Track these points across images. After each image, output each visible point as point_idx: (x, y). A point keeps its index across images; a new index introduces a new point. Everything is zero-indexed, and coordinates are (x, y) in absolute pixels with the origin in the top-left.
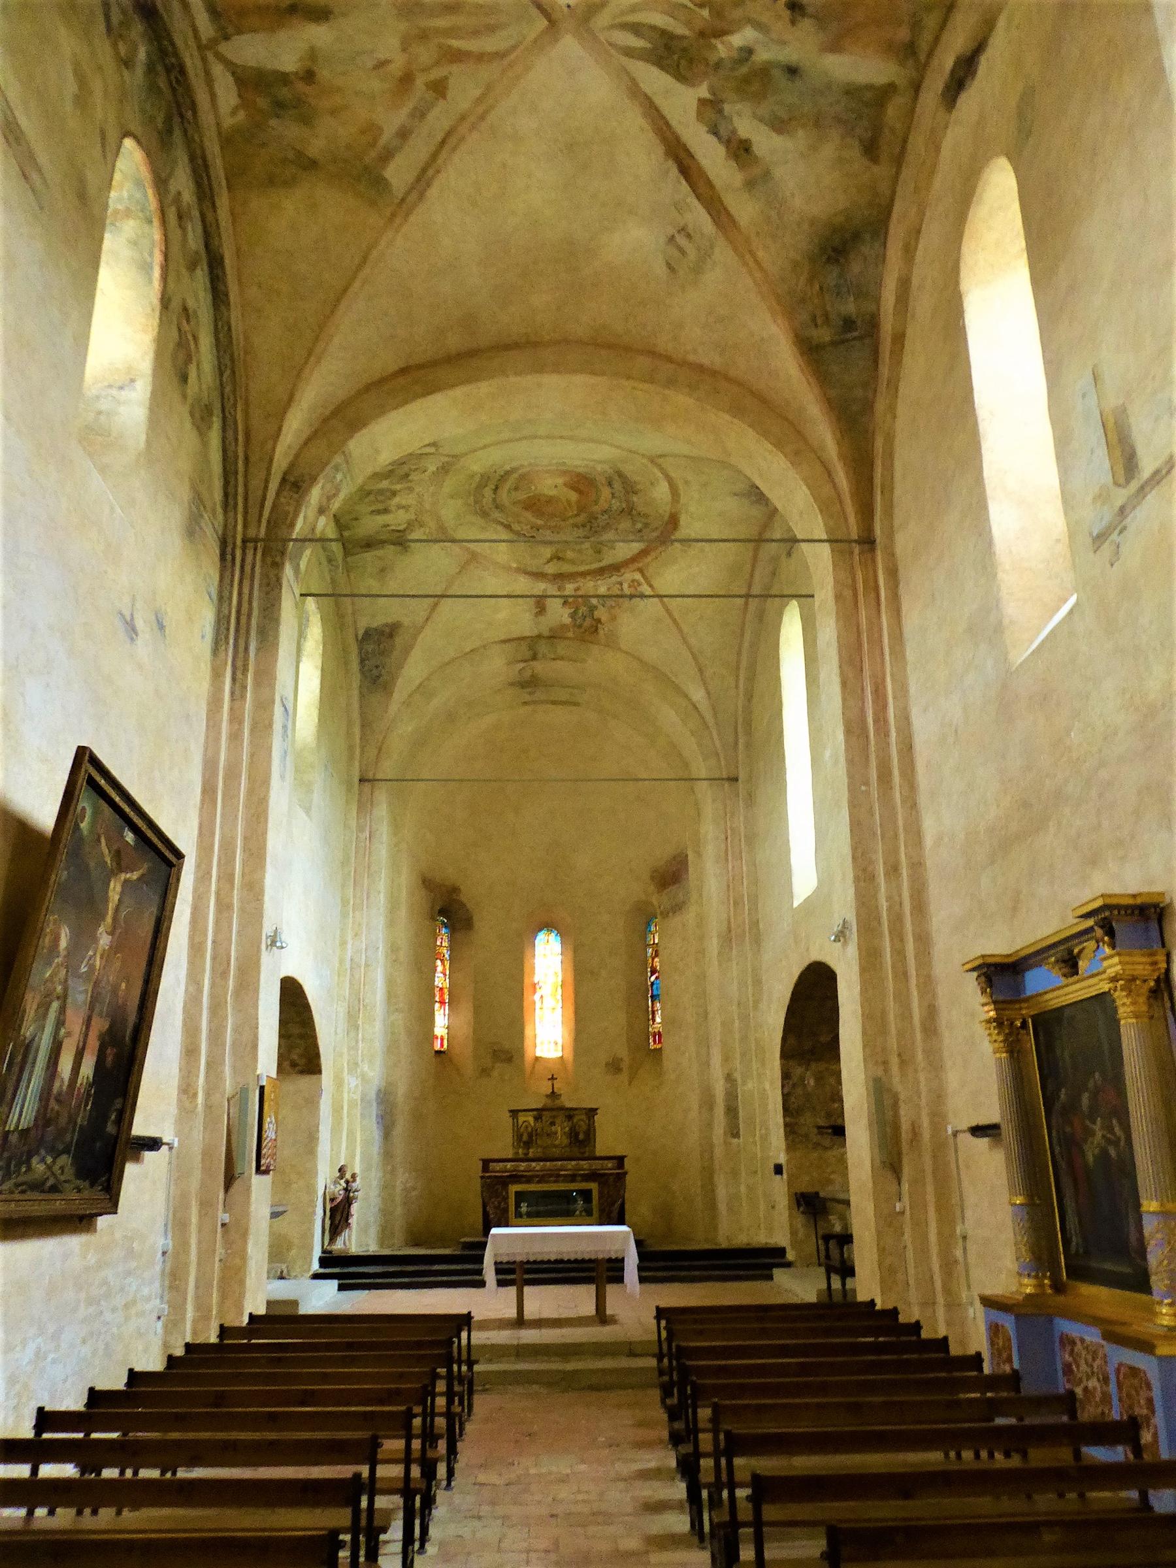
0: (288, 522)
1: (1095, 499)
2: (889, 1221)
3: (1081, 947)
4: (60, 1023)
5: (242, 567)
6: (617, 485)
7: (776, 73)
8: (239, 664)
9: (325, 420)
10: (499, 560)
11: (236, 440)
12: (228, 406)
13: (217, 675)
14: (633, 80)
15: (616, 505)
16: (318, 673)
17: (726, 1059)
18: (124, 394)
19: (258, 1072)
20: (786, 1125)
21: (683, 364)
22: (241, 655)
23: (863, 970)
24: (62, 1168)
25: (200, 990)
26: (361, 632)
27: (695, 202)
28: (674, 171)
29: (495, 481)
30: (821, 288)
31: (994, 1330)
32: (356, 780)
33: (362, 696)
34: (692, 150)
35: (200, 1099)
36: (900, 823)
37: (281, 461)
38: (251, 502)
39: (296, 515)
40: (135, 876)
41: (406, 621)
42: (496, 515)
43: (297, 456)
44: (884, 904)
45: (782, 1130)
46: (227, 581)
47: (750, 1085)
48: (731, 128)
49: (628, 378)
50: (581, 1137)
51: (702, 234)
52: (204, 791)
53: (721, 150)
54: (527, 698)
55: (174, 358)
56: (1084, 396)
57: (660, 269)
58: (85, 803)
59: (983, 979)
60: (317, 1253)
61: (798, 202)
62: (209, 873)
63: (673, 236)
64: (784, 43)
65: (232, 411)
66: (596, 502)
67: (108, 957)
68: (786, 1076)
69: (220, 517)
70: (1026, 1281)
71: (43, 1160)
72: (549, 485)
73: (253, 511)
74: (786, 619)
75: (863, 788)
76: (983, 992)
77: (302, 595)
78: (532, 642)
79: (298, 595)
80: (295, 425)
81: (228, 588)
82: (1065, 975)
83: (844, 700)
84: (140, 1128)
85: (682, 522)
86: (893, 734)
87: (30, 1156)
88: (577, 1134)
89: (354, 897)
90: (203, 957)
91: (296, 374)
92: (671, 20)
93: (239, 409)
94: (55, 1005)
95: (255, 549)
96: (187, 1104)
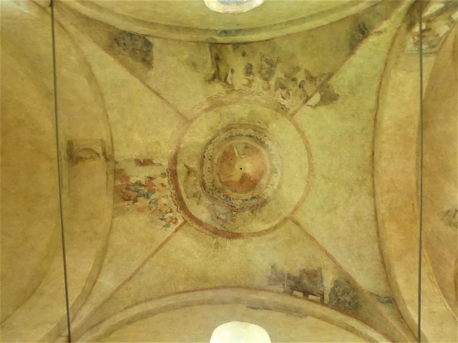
6: (254, 202)
10: (185, 137)
26: (151, 40)
33: (108, 26)
41: (152, 73)
42: (223, 136)
57: (446, 208)
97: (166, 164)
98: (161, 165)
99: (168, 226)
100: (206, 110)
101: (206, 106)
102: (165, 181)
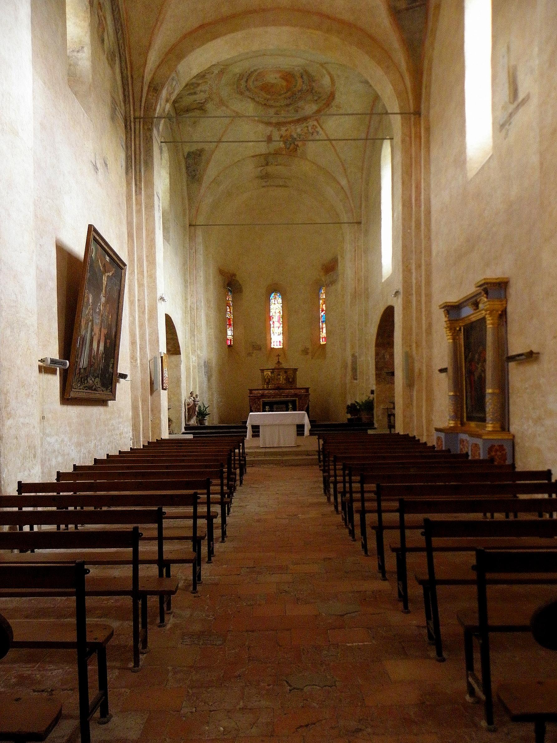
0: (153, 108)
1: (503, 107)
2: (408, 405)
3: (480, 298)
4: (92, 330)
5: (135, 133)
8: (138, 178)
9: (167, 54)
11: (127, 68)
12: (121, 51)
13: (128, 184)
15: (305, 87)
16: (168, 176)
17: (353, 347)
18: (80, 55)
19: (160, 351)
20: (376, 374)
21: (335, 19)
22: (138, 174)
23: (404, 309)
24: (97, 382)
25: (134, 319)
26: (186, 154)
29: (246, 76)
31: (439, 439)
32: (188, 226)
33: (188, 185)
35: (138, 361)
36: (423, 246)
37: (148, 78)
38: (136, 99)
39: (156, 105)
40: (110, 274)
42: (247, 93)
43: (154, 74)
44: (414, 281)
45: (374, 377)
46: (129, 139)
47: (363, 358)
49: (309, 28)
50: (291, 380)
52: (128, 236)
54: (264, 184)
55: (98, 32)
56: (503, 57)
58: (93, 247)
59: (446, 311)
60: (183, 425)
62: (134, 271)
65: (124, 53)
66: (295, 86)
67: (105, 306)
68: (377, 354)
69: (123, 108)
70: (451, 422)
71: (91, 379)
72: (272, 78)
73: (137, 104)
74: (384, 146)
75: (409, 231)
76: (446, 316)
77: (161, 142)
78: (266, 156)
79: (159, 142)
80: (153, 58)
81: (130, 142)
82: (475, 310)
83: (403, 191)
84: (120, 371)
85: (336, 96)
86: (423, 207)
87: (87, 377)
88: (289, 379)
89: (190, 279)
90: (134, 305)
91: (152, 32)
93: (127, 51)
94: (90, 323)
95: (140, 122)
96: (134, 364)
97: (270, 129)
98: (271, 131)
99: (318, 132)
100: (227, 107)
101: (224, 108)
102: (283, 129)
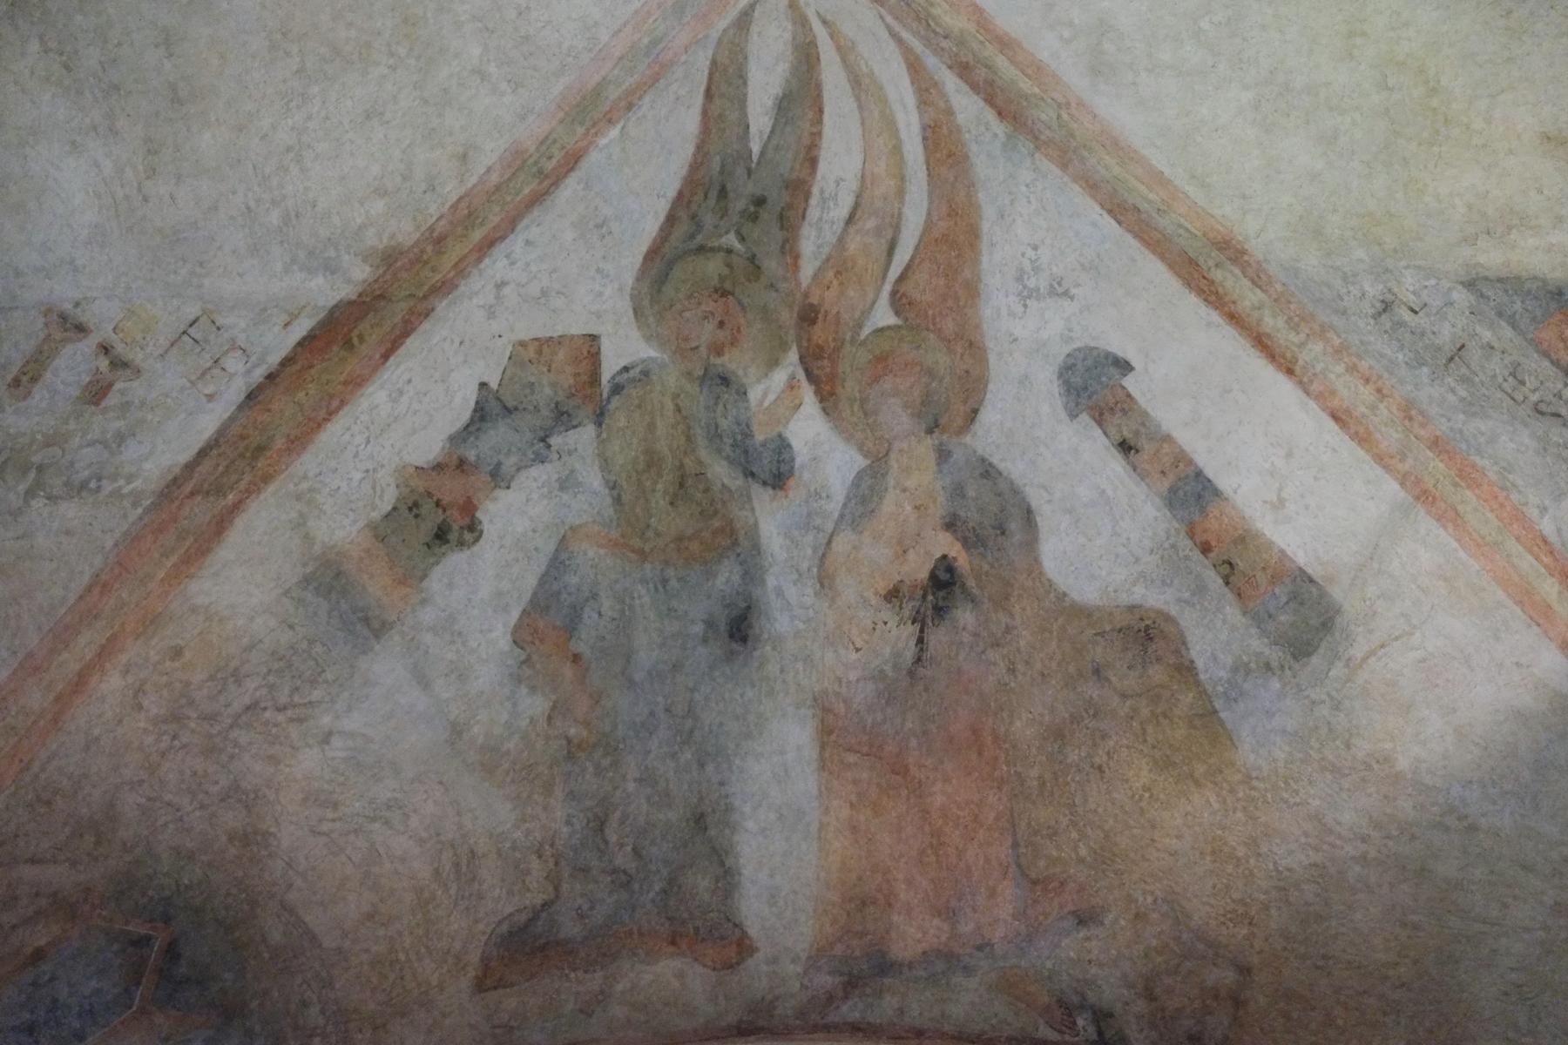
7: (727, 576)
14: (629, 104)
27: (235, 392)
28: (325, 292)
30: (38, 955)
34: (412, 343)
48: (510, 463)
51: (121, 438)
53: (428, 446)
61: (308, 762)
63: (81, 329)
64: (825, 581)
92: (841, 211)
